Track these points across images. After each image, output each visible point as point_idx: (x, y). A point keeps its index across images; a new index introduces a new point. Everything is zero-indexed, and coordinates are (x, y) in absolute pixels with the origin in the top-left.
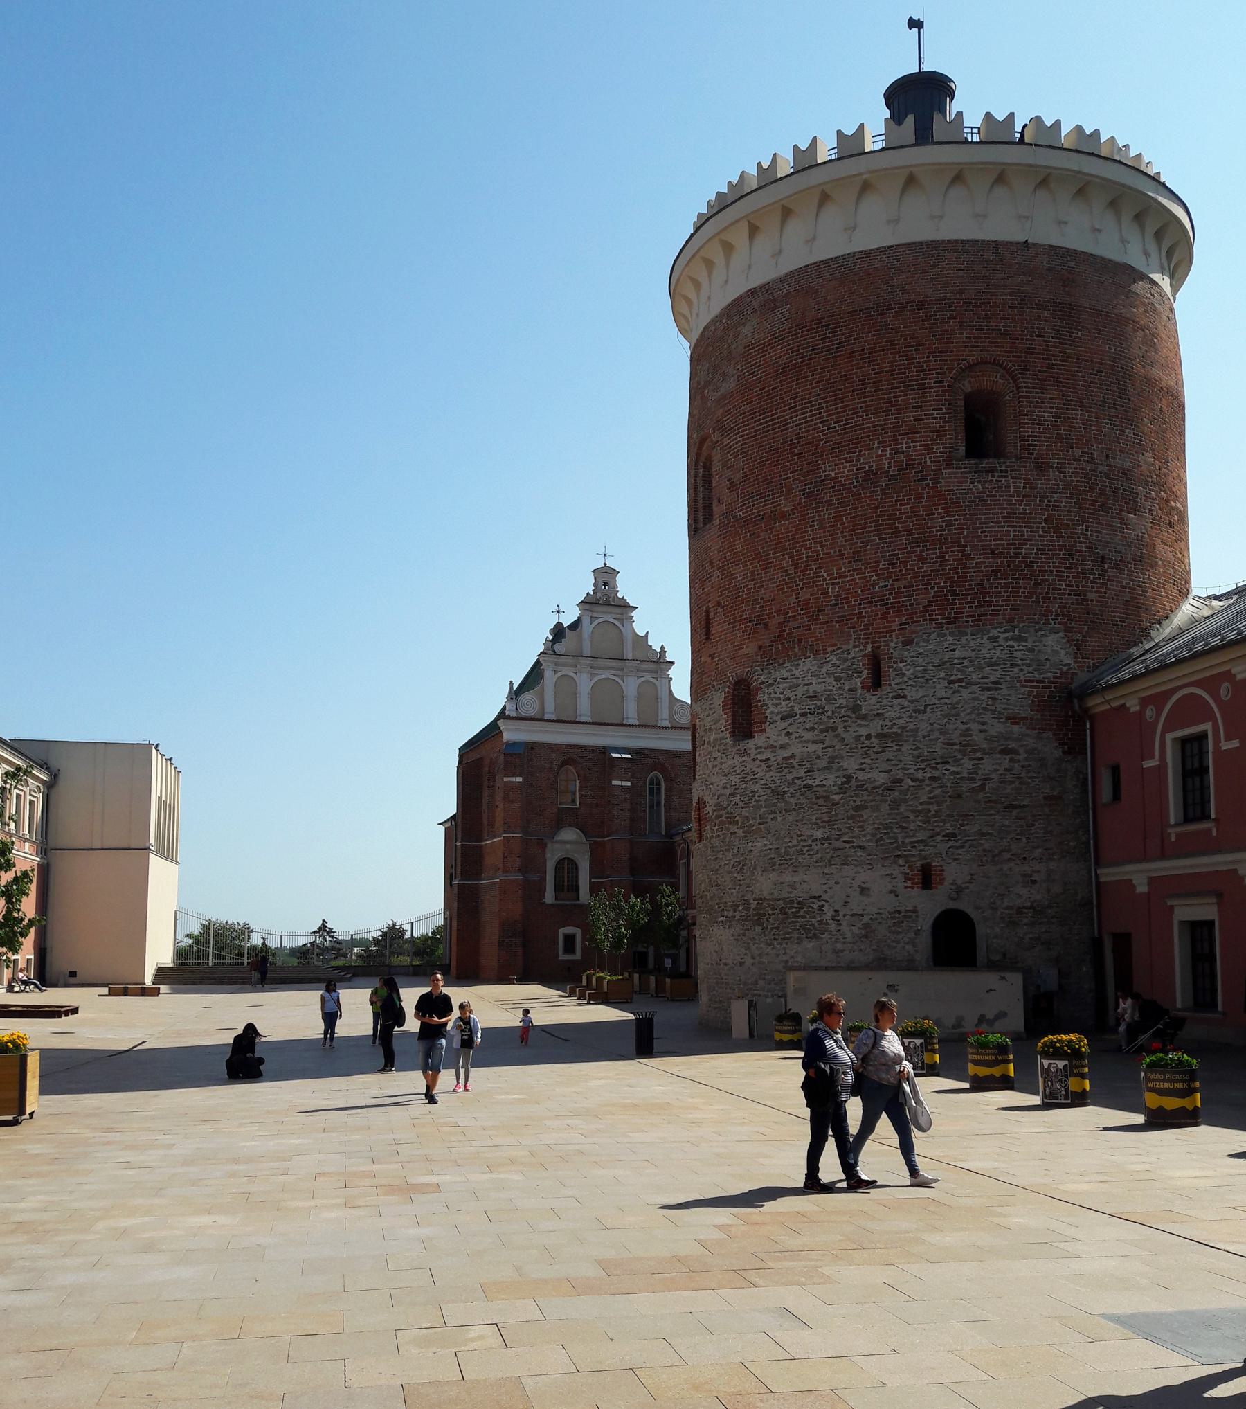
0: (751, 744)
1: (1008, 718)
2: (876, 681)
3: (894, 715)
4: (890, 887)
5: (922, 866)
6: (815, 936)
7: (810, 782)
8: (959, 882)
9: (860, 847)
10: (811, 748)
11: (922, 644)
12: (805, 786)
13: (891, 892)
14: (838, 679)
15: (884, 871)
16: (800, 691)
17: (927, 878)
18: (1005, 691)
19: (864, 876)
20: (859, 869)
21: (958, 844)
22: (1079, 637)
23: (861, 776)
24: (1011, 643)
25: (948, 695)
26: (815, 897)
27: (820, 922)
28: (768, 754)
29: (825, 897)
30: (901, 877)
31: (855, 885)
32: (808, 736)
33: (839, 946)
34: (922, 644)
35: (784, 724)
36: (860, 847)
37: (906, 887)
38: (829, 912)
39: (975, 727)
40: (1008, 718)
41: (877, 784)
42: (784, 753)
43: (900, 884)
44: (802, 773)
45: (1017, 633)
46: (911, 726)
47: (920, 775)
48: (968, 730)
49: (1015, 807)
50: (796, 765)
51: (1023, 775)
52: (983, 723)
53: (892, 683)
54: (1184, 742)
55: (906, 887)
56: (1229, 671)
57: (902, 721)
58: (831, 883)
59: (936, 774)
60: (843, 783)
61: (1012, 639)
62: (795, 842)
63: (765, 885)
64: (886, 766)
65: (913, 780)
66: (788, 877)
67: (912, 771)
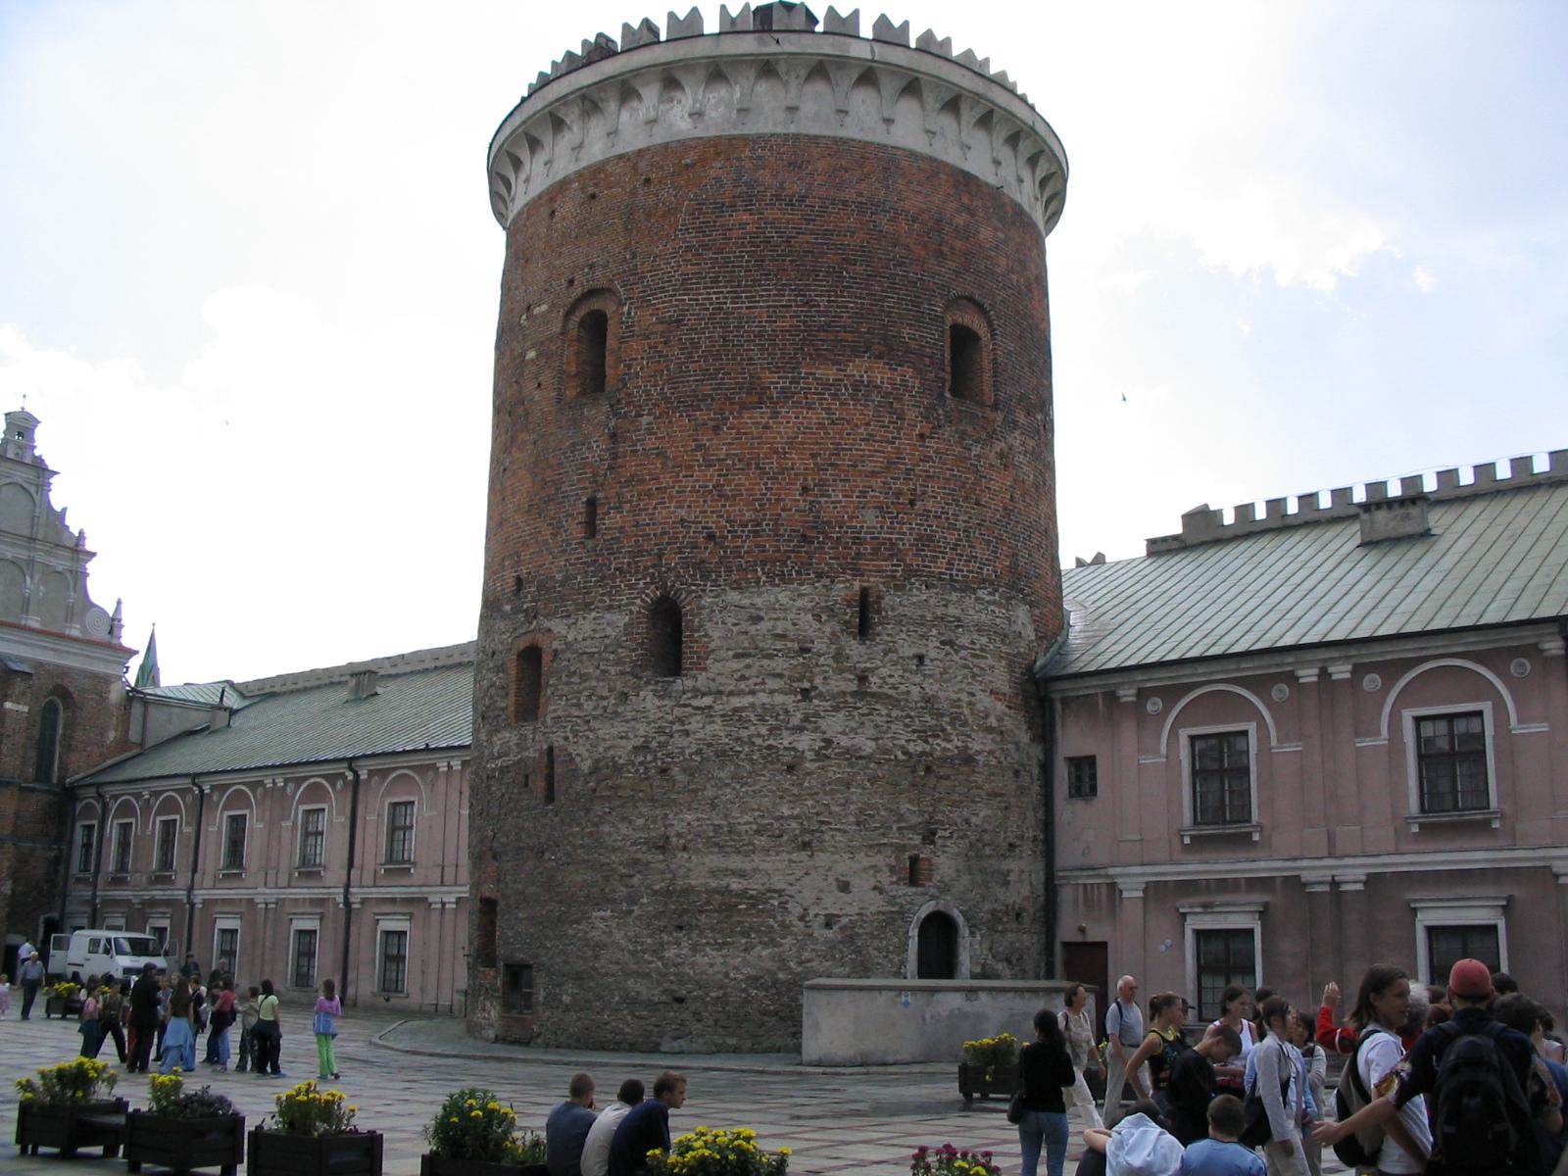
0: (679, 684)
1: (992, 692)
2: (864, 629)
3: (884, 672)
4: (873, 882)
5: (910, 858)
6: (772, 940)
7: (774, 743)
8: (946, 879)
9: (839, 830)
10: (779, 698)
11: (915, 591)
12: (770, 747)
13: (875, 888)
14: (817, 617)
15: (867, 862)
16: (764, 626)
17: (914, 873)
18: (990, 661)
19: (844, 866)
20: (837, 857)
21: (947, 834)
22: (1037, 612)
23: (845, 742)
24: (991, 608)
25: (941, 656)
26: (775, 891)
27: (784, 926)
28: (707, 701)
29: (791, 890)
30: (885, 869)
31: (831, 879)
32: (773, 684)
33: (806, 955)
34: (915, 591)
35: (736, 665)
36: (839, 830)
37: (892, 883)
38: (796, 910)
39: (965, 697)
40: (992, 692)
41: (864, 753)
42: (736, 702)
43: (885, 878)
44: (764, 731)
45: (997, 598)
46: (903, 688)
47: (911, 748)
48: (959, 700)
49: (996, 795)
50: (753, 718)
51: (1003, 759)
52: (973, 695)
53: (884, 632)
54: (1193, 739)
55: (892, 883)
56: (1292, 672)
57: (892, 681)
58: (799, 874)
59: (928, 749)
60: (821, 748)
61: (994, 603)
62: (746, 818)
63: (699, 870)
64: (872, 732)
65: (904, 753)
66: (735, 862)
67: (903, 742)
